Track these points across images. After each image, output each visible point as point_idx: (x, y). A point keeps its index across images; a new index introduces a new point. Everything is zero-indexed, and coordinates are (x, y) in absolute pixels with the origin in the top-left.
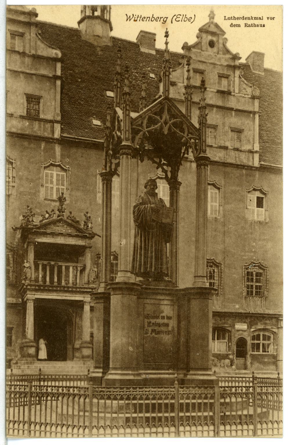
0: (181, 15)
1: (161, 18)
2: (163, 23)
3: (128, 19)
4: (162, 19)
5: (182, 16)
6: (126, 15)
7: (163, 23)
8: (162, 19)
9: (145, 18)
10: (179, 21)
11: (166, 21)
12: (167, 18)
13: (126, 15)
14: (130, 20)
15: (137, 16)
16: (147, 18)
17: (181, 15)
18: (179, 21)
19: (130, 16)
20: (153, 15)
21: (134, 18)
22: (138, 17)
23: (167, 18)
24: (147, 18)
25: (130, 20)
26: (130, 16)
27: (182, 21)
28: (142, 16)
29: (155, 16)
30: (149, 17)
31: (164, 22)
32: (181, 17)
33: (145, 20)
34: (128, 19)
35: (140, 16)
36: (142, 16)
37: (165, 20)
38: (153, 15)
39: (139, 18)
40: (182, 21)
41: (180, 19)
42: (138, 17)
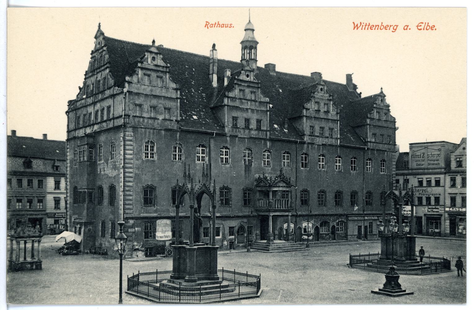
0: (422, 23)
1: (390, 26)
2: (393, 32)
3: (356, 27)
4: (392, 28)
5: (424, 24)
6: (354, 23)
7: (393, 32)
8: (392, 28)
9: (374, 26)
10: (421, 29)
11: (396, 29)
12: (397, 26)
13: (354, 23)
14: (357, 29)
15: (365, 24)
16: (376, 26)
17: (422, 23)
18: (421, 29)
19: (357, 26)
20: (382, 23)
21: (361, 26)
22: (366, 25)
23: (397, 26)
24: (376, 26)
25: (357, 29)
26: (357, 26)
27: (424, 29)
28: (371, 25)
29: (385, 24)
30: (378, 26)
31: (394, 31)
32: (423, 25)
33: (374, 28)
34: (356, 27)
35: (368, 24)
36: (371, 25)
37: (395, 28)
38: (382, 23)
39: (367, 27)
40: (424, 29)
41: (422, 27)
42: (366, 25)
